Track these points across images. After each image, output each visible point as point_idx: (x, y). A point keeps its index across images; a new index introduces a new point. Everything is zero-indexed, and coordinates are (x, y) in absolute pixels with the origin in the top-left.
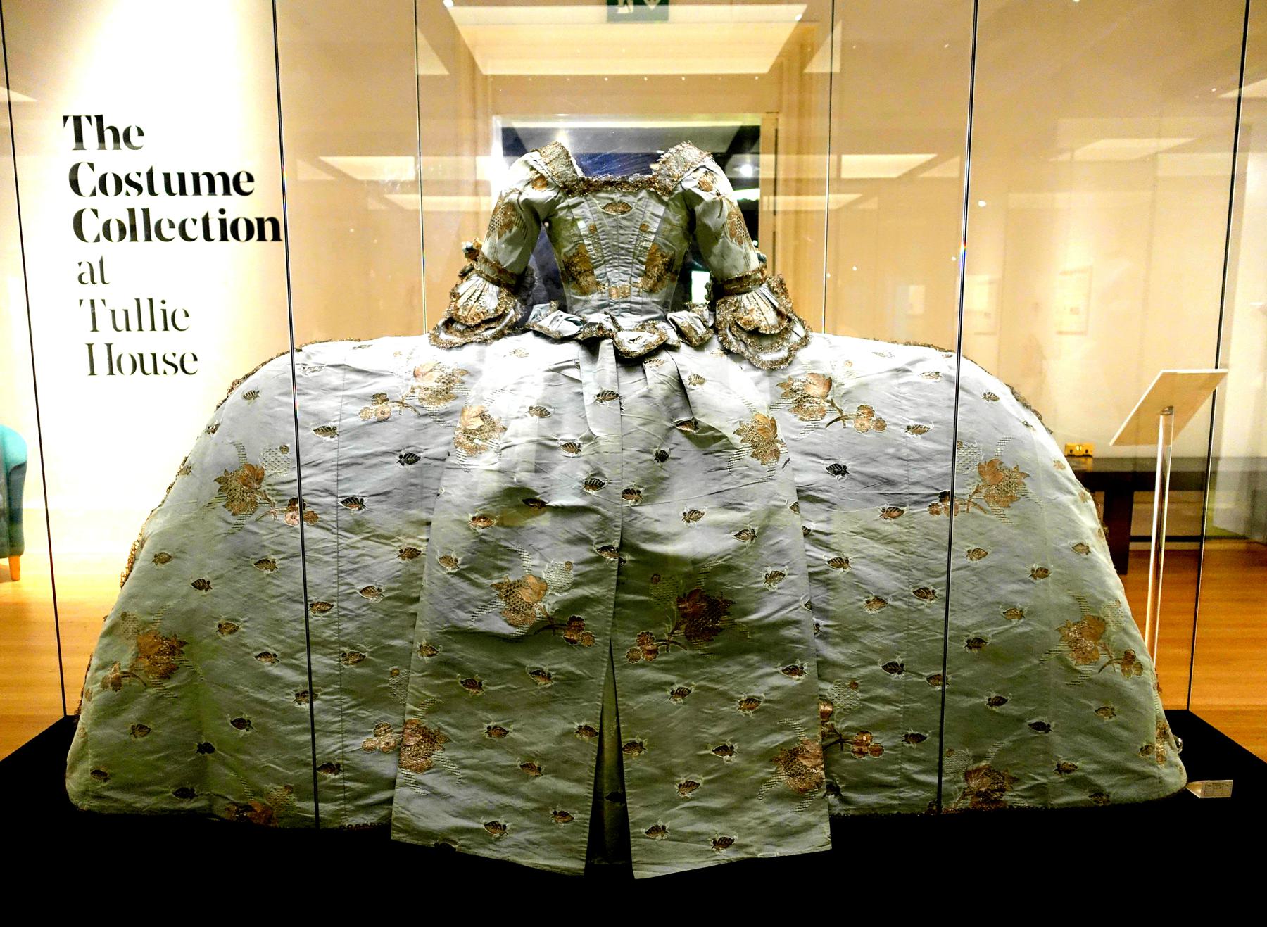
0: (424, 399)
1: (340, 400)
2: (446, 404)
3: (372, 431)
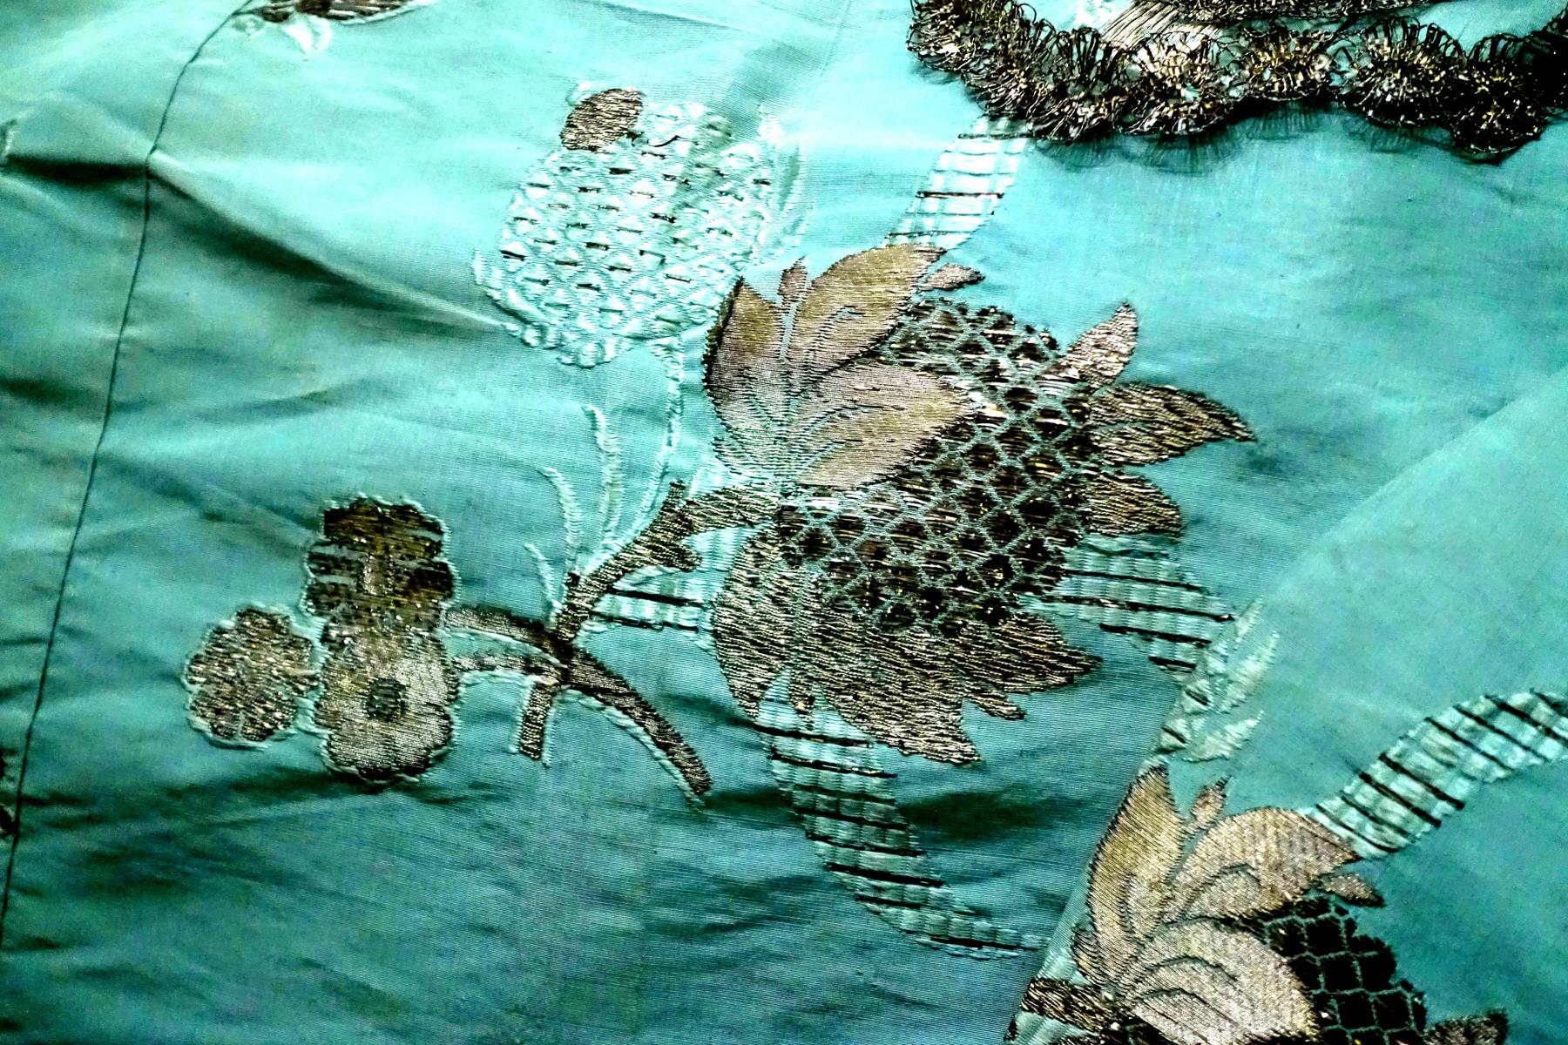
0: (763, 646)
1: (65, 494)
2: (972, 720)
3: (274, 849)
